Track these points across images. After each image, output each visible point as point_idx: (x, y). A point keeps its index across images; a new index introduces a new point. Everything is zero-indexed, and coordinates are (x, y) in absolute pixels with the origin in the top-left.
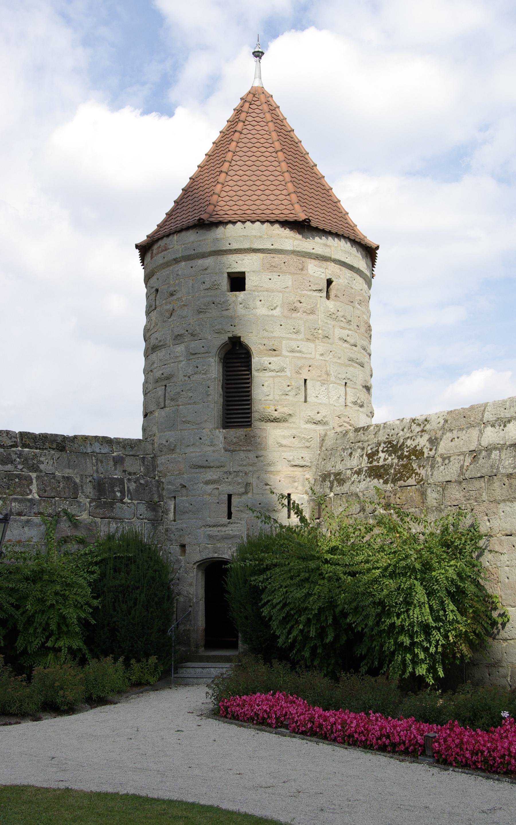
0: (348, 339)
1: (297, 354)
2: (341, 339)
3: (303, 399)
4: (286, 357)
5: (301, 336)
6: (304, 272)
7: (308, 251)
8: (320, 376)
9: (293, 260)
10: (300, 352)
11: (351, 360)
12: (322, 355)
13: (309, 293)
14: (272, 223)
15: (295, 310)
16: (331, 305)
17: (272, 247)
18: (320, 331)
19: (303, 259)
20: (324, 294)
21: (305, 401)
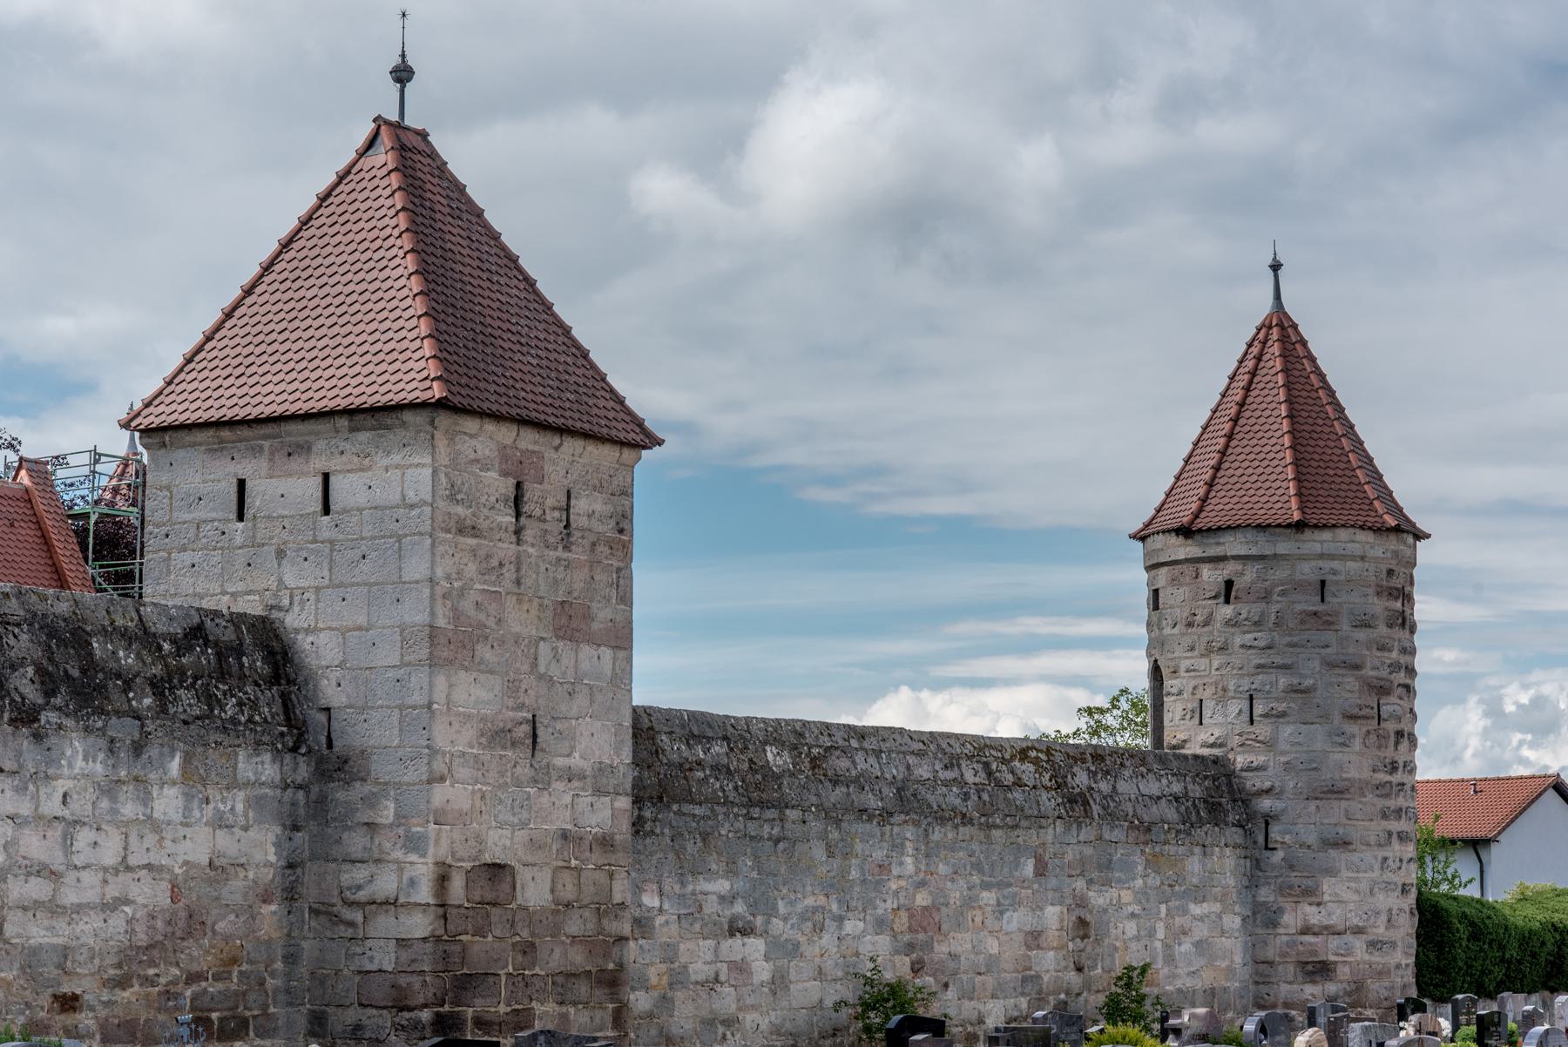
0: (1256, 643)
1: (1192, 674)
2: (1242, 646)
3: (1197, 721)
4: (1184, 678)
5: (1196, 653)
6: (1198, 580)
7: (1199, 555)
8: (1215, 694)
9: (1189, 569)
10: (1194, 670)
11: (1259, 666)
12: (1217, 669)
13: (1204, 602)
14: (1169, 531)
15: (1190, 625)
16: (1227, 611)
17: (1170, 559)
18: (1214, 644)
19: (1197, 565)
20: (1222, 599)
21: (1201, 723)
